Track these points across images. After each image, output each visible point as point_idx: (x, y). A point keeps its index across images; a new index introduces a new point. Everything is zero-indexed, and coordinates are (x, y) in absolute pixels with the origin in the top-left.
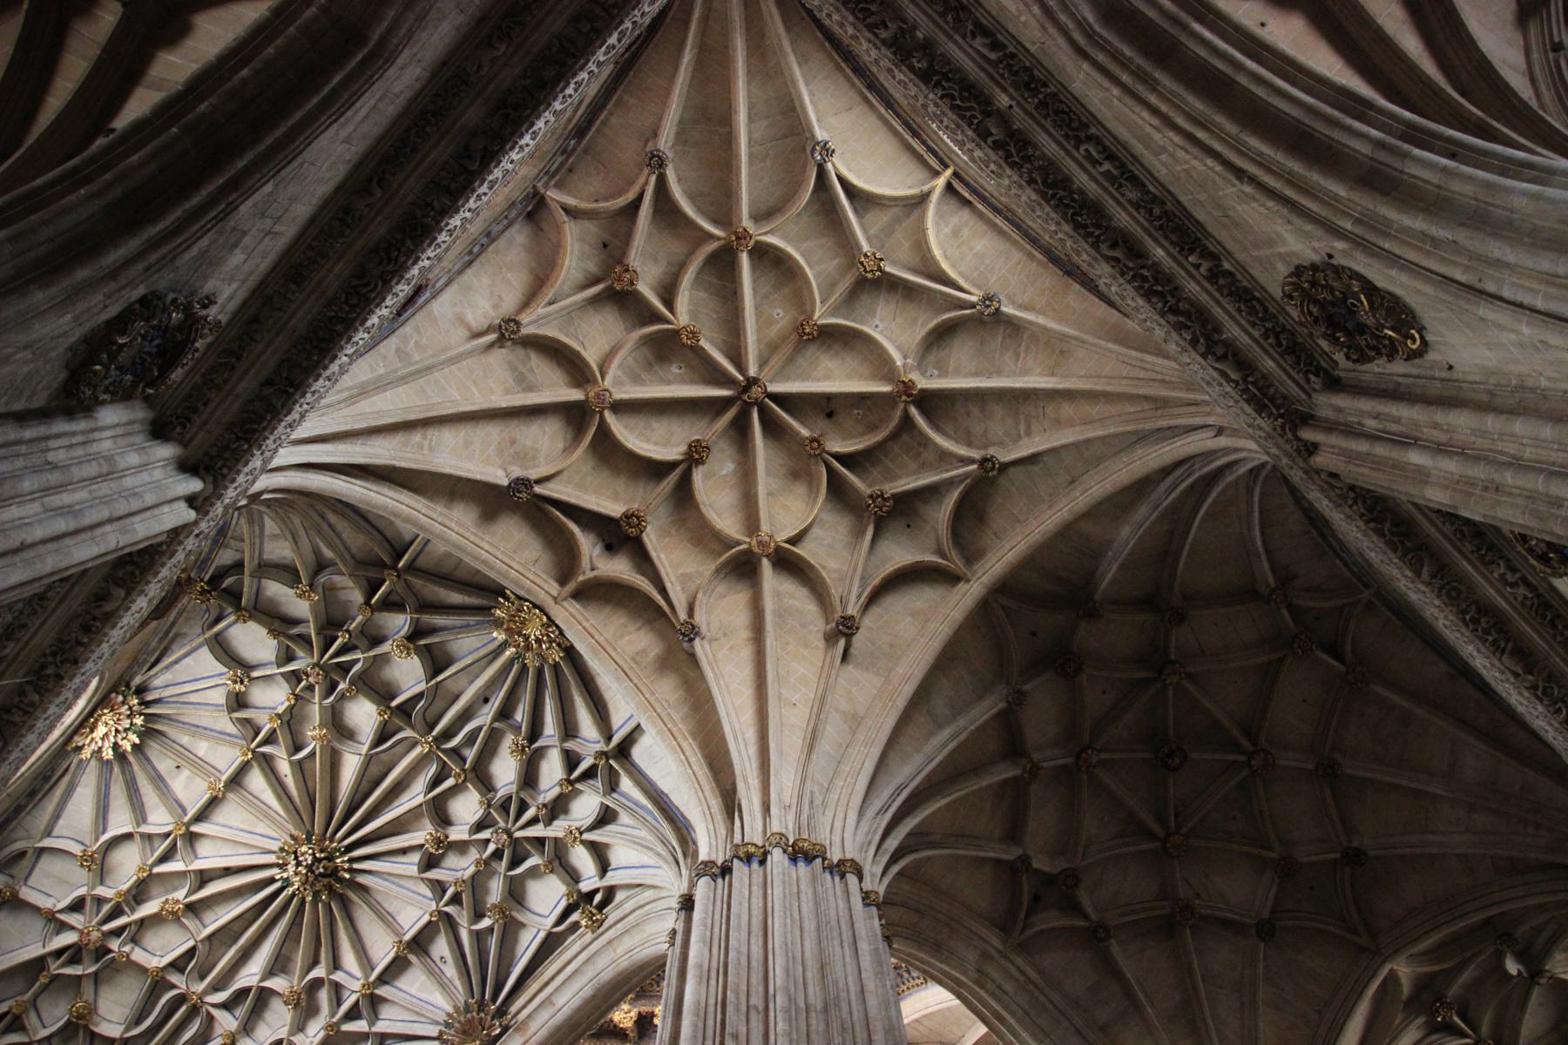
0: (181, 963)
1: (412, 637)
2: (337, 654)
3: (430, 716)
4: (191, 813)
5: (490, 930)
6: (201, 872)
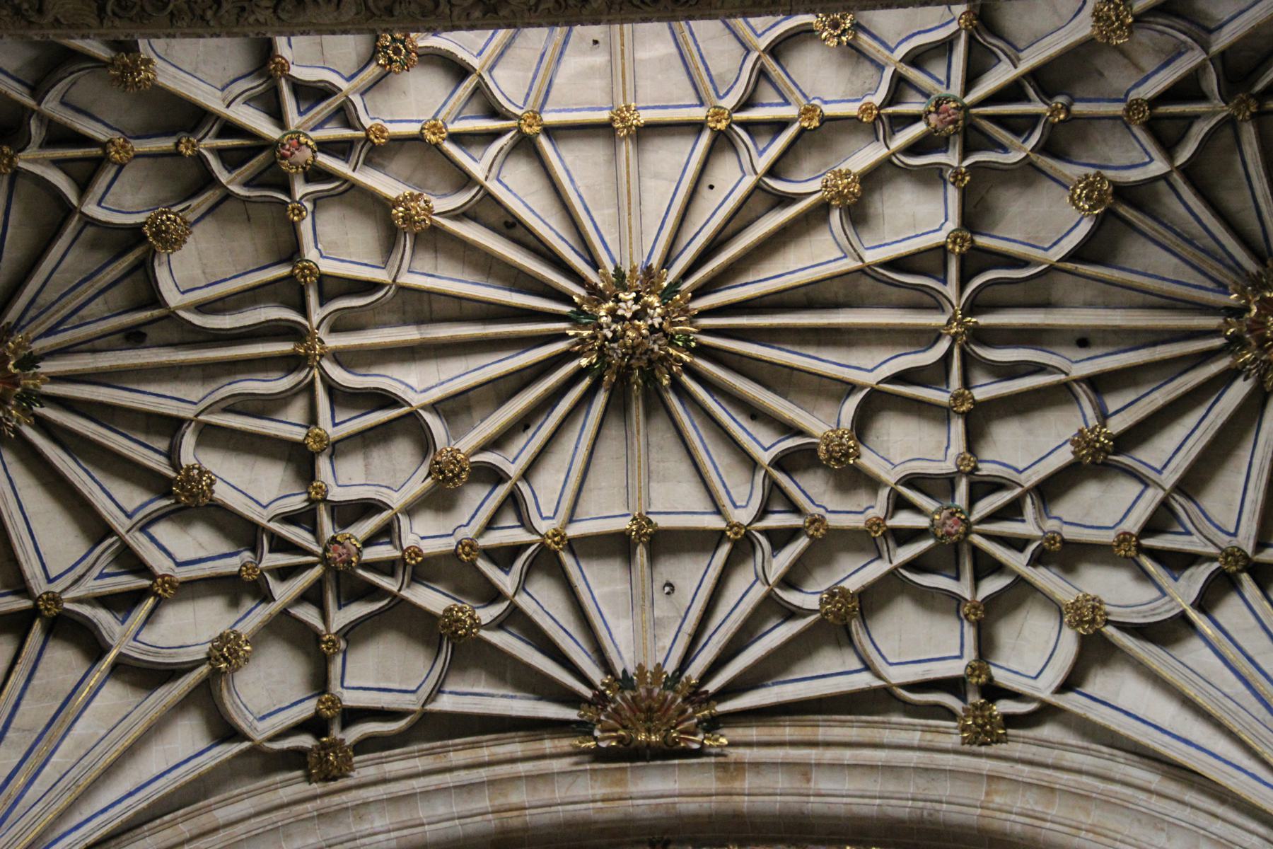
0: (328, 286)
1: (1123, 192)
2: (997, 120)
3: (987, 295)
4: (550, 118)
5: (792, 613)
6: (489, 196)
